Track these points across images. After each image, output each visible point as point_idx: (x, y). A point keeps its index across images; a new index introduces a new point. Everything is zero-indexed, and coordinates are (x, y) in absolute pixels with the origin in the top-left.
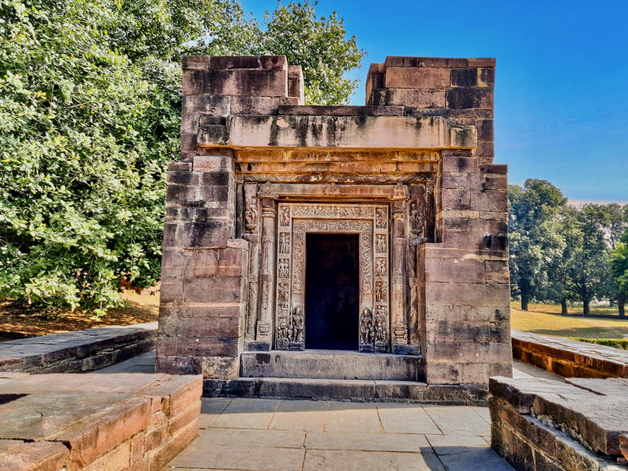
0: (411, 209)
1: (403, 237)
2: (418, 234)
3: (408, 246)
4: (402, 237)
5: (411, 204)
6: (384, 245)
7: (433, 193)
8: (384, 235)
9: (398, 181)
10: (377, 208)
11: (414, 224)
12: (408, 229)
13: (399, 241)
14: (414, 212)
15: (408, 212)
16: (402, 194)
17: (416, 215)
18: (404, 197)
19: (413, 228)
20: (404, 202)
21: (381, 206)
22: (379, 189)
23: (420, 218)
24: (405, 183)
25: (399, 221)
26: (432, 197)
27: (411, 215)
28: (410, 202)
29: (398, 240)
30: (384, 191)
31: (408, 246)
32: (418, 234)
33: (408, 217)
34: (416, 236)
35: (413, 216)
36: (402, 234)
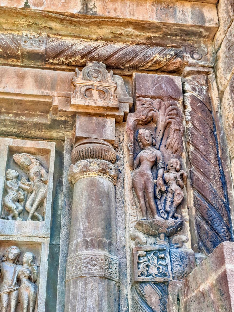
0: (138, 144)
1: (109, 246)
2: (169, 236)
3: (127, 291)
4: (101, 245)
5: (135, 129)
6: (27, 290)
7: (209, 99)
8: (34, 247)
9: (87, 55)
10: (12, 151)
11: (151, 199)
12: (129, 216)
13: (92, 261)
14: (148, 154)
15: (125, 157)
16: (103, 93)
17: (155, 165)
18: (112, 103)
19: (148, 210)
20: (110, 123)
21: (30, 144)
22: (22, 77)
23: (171, 175)
24: (113, 65)
25: (92, 184)
26: (205, 107)
27: (136, 164)
28: (131, 120)
29: (82, 257)
30: (40, 82)
31: (127, 291)
32: (169, 236)
33: (128, 174)
34: (162, 243)
35: (146, 167)
36: (106, 239)
